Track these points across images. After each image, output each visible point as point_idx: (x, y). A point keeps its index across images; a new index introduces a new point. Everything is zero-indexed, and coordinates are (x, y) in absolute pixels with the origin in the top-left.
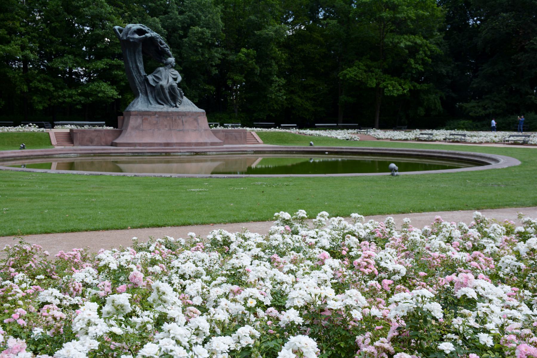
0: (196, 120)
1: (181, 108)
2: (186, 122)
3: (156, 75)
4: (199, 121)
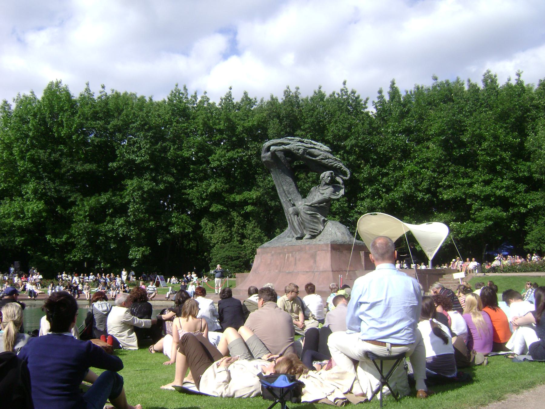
0: (313, 256)
2: (299, 260)
4: (318, 258)
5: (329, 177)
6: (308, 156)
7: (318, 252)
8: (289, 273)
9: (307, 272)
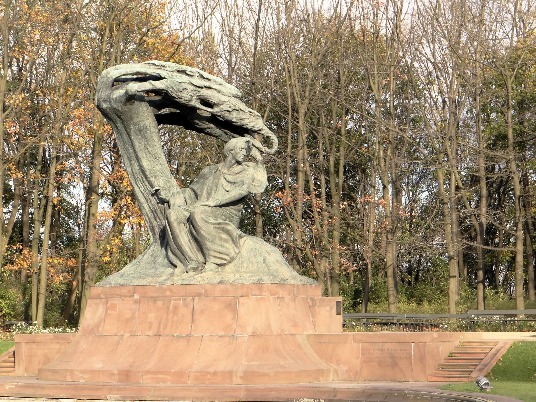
0: (232, 307)
1: (210, 275)
2: (202, 311)
3: (195, 188)
4: (242, 311)
5: (243, 148)
6: (198, 105)
7: (242, 300)
8: (179, 337)
9: (220, 336)
